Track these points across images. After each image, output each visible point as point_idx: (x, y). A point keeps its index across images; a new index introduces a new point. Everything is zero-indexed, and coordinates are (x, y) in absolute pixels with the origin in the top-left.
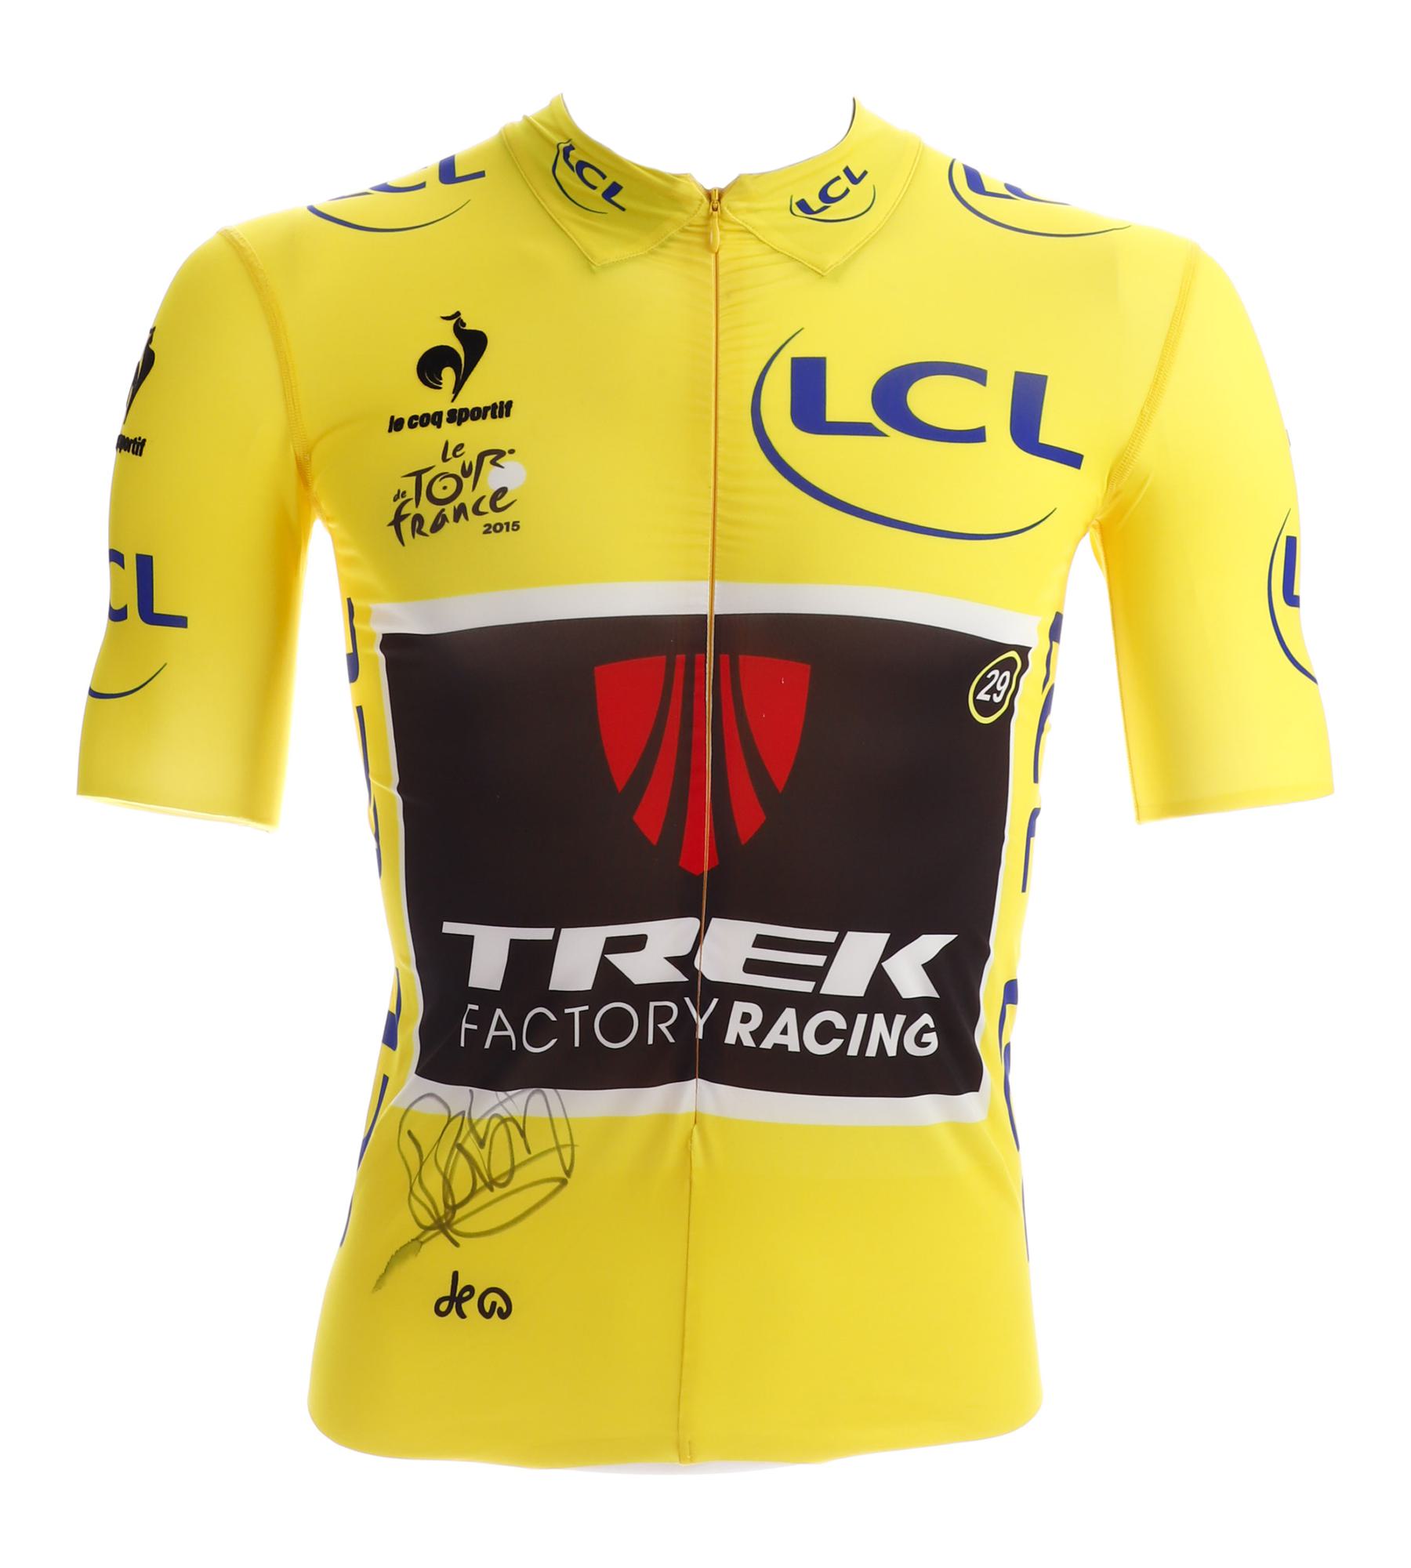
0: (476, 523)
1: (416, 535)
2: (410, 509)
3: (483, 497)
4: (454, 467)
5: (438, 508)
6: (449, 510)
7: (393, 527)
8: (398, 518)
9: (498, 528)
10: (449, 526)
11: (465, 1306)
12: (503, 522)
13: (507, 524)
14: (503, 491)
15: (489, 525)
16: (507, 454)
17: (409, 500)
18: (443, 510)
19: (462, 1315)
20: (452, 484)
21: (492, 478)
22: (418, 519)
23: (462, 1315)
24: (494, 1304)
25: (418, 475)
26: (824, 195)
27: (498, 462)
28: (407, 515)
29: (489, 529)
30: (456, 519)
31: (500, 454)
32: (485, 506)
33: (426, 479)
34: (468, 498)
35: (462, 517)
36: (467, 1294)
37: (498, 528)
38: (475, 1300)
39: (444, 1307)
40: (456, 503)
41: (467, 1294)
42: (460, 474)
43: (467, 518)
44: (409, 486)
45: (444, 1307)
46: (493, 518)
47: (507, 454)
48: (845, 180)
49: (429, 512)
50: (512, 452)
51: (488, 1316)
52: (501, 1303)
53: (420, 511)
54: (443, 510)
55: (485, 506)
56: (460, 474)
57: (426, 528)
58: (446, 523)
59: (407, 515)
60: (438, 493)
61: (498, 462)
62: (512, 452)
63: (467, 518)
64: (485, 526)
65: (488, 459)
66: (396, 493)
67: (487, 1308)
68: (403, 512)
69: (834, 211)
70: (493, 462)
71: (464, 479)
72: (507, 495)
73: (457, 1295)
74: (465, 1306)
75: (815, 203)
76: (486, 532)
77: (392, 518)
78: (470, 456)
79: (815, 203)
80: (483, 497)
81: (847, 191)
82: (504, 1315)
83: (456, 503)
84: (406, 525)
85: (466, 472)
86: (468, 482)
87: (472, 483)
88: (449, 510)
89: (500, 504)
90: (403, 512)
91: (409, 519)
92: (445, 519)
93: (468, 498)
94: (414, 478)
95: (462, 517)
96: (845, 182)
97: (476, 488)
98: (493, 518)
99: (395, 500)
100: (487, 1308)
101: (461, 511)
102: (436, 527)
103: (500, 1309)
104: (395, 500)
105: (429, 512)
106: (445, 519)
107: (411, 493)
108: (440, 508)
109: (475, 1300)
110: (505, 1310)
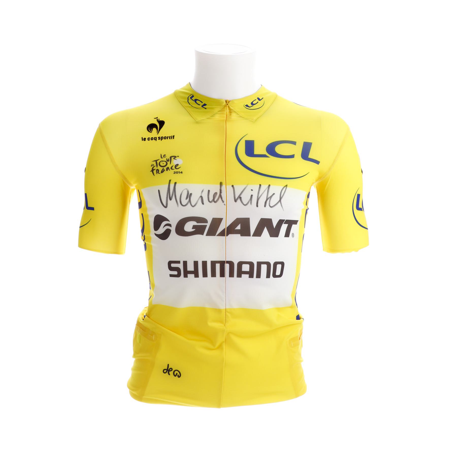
0: (172, 171)
1: (158, 174)
2: (155, 168)
3: (173, 166)
4: (165, 159)
5: (162, 168)
6: (165, 168)
7: (152, 172)
8: (152, 170)
9: (177, 172)
10: (165, 172)
11: (170, 372)
12: (178, 171)
13: (179, 172)
14: (178, 165)
15: (175, 172)
16: (177, 157)
17: (155, 166)
18: (164, 168)
19: (169, 374)
20: (165, 164)
21: (174, 162)
22: (158, 170)
23: (169, 374)
24: (177, 374)
25: (156, 161)
26: (252, 104)
27: (175, 158)
28: (155, 169)
29: (175, 173)
30: (167, 170)
31: (175, 157)
32: (173, 168)
33: (158, 162)
34: (169, 166)
35: (168, 170)
36: (171, 370)
37: (177, 172)
38: (172, 371)
39: (165, 371)
40: (167, 167)
41: (171, 370)
42: (166, 161)
43: (169, 170)
44: (154, 163)
45: (165, 371)
46: (176, 170)
47: (177, 157)
48: (257, 100)
49: (160, 169)
50: (178, 156)
51: (175, 376)
52: (178, 374)
53: (158, 168)
54: (164, 168)
55: (173, 168)
56: (166, 161)
57: (160, 172)
58: (165, 171)
59: (155, 169)
60: (161, 164)
61: (175, 158)
62: (178, 156)
63: (169, 170)
64: (174, 172)
65: (172, 158)
66: (151, 165)
67: (175, 374)
68: (154, 169)
69: (255, 107)
70: (174, 159)
71: (168, 162)
72: (178, 166)
73: (168, 369)
74: (170, 372)
75: (250, 105)
76: (174, 173)
77: (151, 170)
78: (168, 157)
79: (250, 105)
80: (173, 166)
81: (258, 102)
82: (179, 377)
83: (167, 167)
84: (155, 172)
85: (168, 161)
86: (169, 163)
87: (170, 163)
88: (165, 168)
89: (177, 167)
90: (154, 169)
91: (155, 170)
92: (164, 170)
93: (169, 166)
94: (155, 162)
95: (168, 170)
96: (257, 100)
97: (171, 163)
98: (176, 170)
99: (151, 166)
100: (175, 374)
101: (168, 169)
102: (162, 172)
103: (178, 375)
104: (151, 166)
105: (160, 169)
106: (164, 170)
107: (155, 165)
108: (162, 168)
109: (172, 371)
110: (179, 375)
